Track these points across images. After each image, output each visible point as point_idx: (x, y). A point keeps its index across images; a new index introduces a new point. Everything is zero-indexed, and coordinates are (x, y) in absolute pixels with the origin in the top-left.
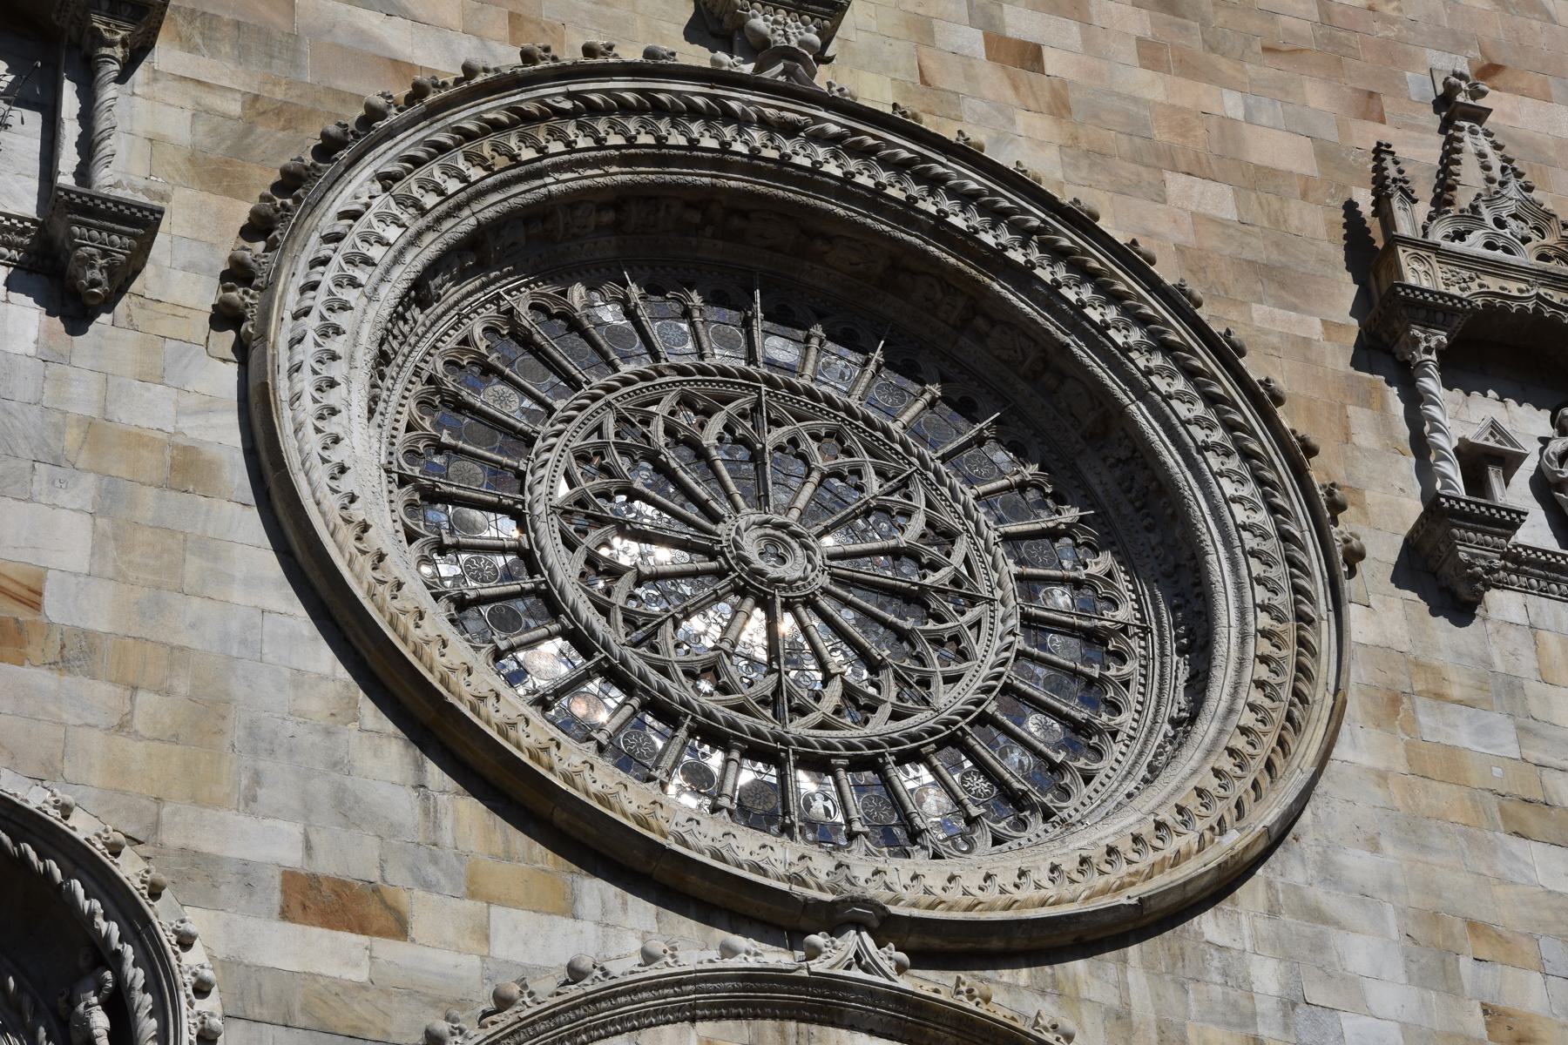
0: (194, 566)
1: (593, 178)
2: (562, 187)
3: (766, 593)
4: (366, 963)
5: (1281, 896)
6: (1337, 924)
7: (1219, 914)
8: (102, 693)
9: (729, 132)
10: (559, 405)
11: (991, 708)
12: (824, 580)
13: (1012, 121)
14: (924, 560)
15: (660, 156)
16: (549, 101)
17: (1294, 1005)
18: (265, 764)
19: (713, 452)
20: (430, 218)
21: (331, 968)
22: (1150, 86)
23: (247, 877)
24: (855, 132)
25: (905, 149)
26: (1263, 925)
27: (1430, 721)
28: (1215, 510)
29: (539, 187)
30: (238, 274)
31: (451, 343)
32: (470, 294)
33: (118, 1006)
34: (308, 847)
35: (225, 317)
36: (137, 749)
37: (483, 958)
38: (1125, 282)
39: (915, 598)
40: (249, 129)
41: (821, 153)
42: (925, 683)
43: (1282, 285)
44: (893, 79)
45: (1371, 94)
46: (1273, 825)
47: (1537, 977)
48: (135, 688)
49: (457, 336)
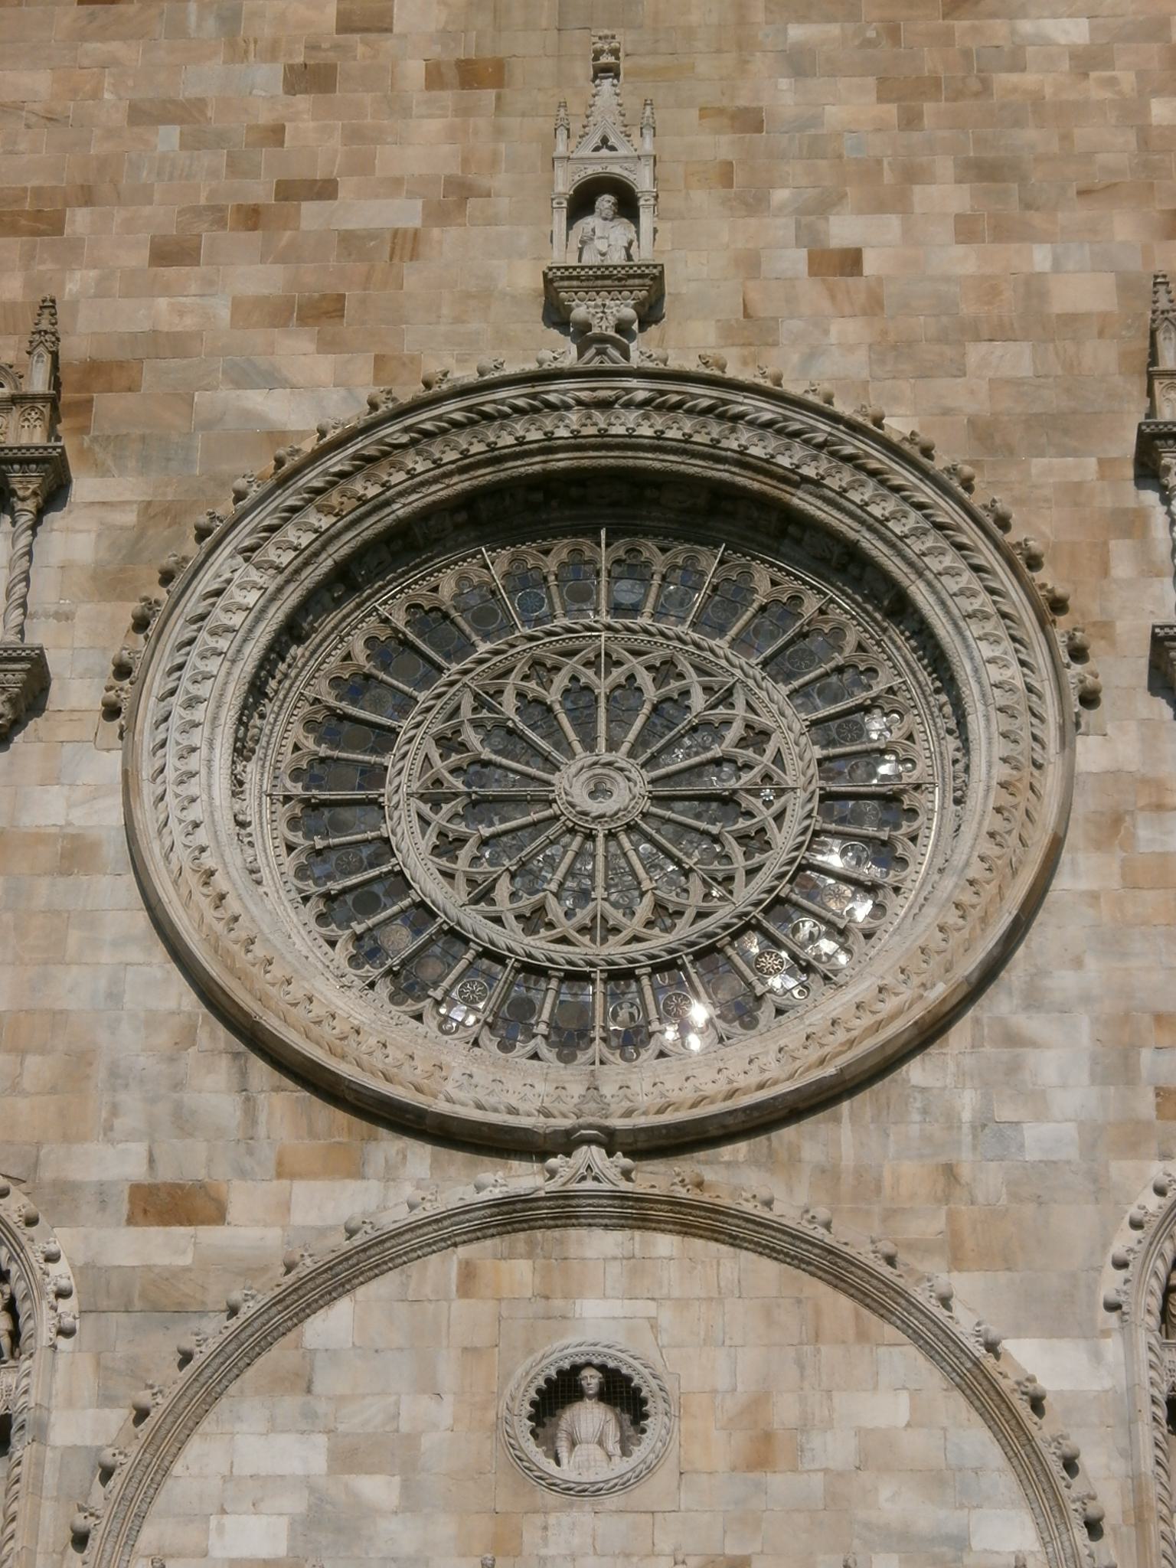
0: (74, 937)
1: (438, 492)
2: (408, 509)
3: (592, 829)
5: (986, 1030)
6: (1033, 1044)
7: (926, 1058)
9: (548, 423)
10: (421, 696)
11: (783, 889)
12: (646, 805)
13: (826, 332)
14: (740, 764)
16: (387, 440)
17: (984, 1126)
18: (122, 1097)
19: (557, 707)
20: (287, 572)
21: (163, 1259)
23: (102, 1195)
24: (662, 393)
25: (705, 396)
28: (976, 670)
29: (388, 515)
30: (122, 671)
31: (334, 661)
32: (348, 615)
34: (151, 1160)
35: (112, 711)
36: (23, 1104)
37: (283, 1227)
38: (902, 475)
41: (632, 417)
44: (719, 321)
46: (971, 973)
48: (22, 1052)
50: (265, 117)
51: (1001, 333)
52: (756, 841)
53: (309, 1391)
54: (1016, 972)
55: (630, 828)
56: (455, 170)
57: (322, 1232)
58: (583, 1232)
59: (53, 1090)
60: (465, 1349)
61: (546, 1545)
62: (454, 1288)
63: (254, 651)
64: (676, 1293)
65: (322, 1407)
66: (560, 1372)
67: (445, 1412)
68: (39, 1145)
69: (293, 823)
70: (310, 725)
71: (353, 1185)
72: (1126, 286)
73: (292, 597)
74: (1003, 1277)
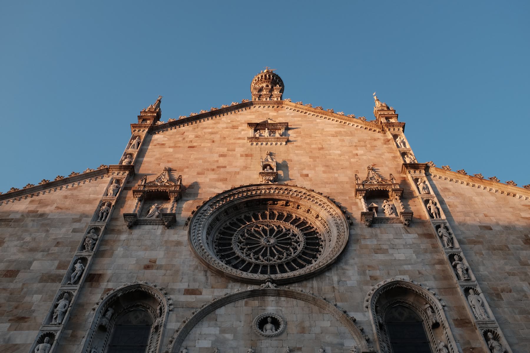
0: (177, 255)
4: (195, 299)
6: (347, 270)
8: (162, 272)
15: (252, 196)
17: (340, 281)
22: (325, 175)
23: (179, 291)
26: (335, 272)
27: (363, 242)
33: (161, 309)
34: (189, 286)
39: (290, 244)
40: (193, 203)
42: (291, 254)
43: (343, 194)
45: (357, 171)
47: (378, 271)
48: (167, 270)
49: (224, 224)
50: (216, 159)
51: (331, 183)
52: (295, 249)
53: (216, 321)
54: (343, 261)
55: (274, 247)
56: (245, 165)
57: (219, 296)
58: (268, 297)
59: (172, 275)
60: (246, 314)
61: (262, 345)
62: (244, 305)
63: (210, 220)
64: (285, 306)
65: (218, 323)
66: (264, 318)
67: (242, 324)
68: (168, 283)
69: (216, 246)
70: (219, 233)
71: (225, 290)
72: (350, 178)
73: (217, 213)
74: (346, 303)
